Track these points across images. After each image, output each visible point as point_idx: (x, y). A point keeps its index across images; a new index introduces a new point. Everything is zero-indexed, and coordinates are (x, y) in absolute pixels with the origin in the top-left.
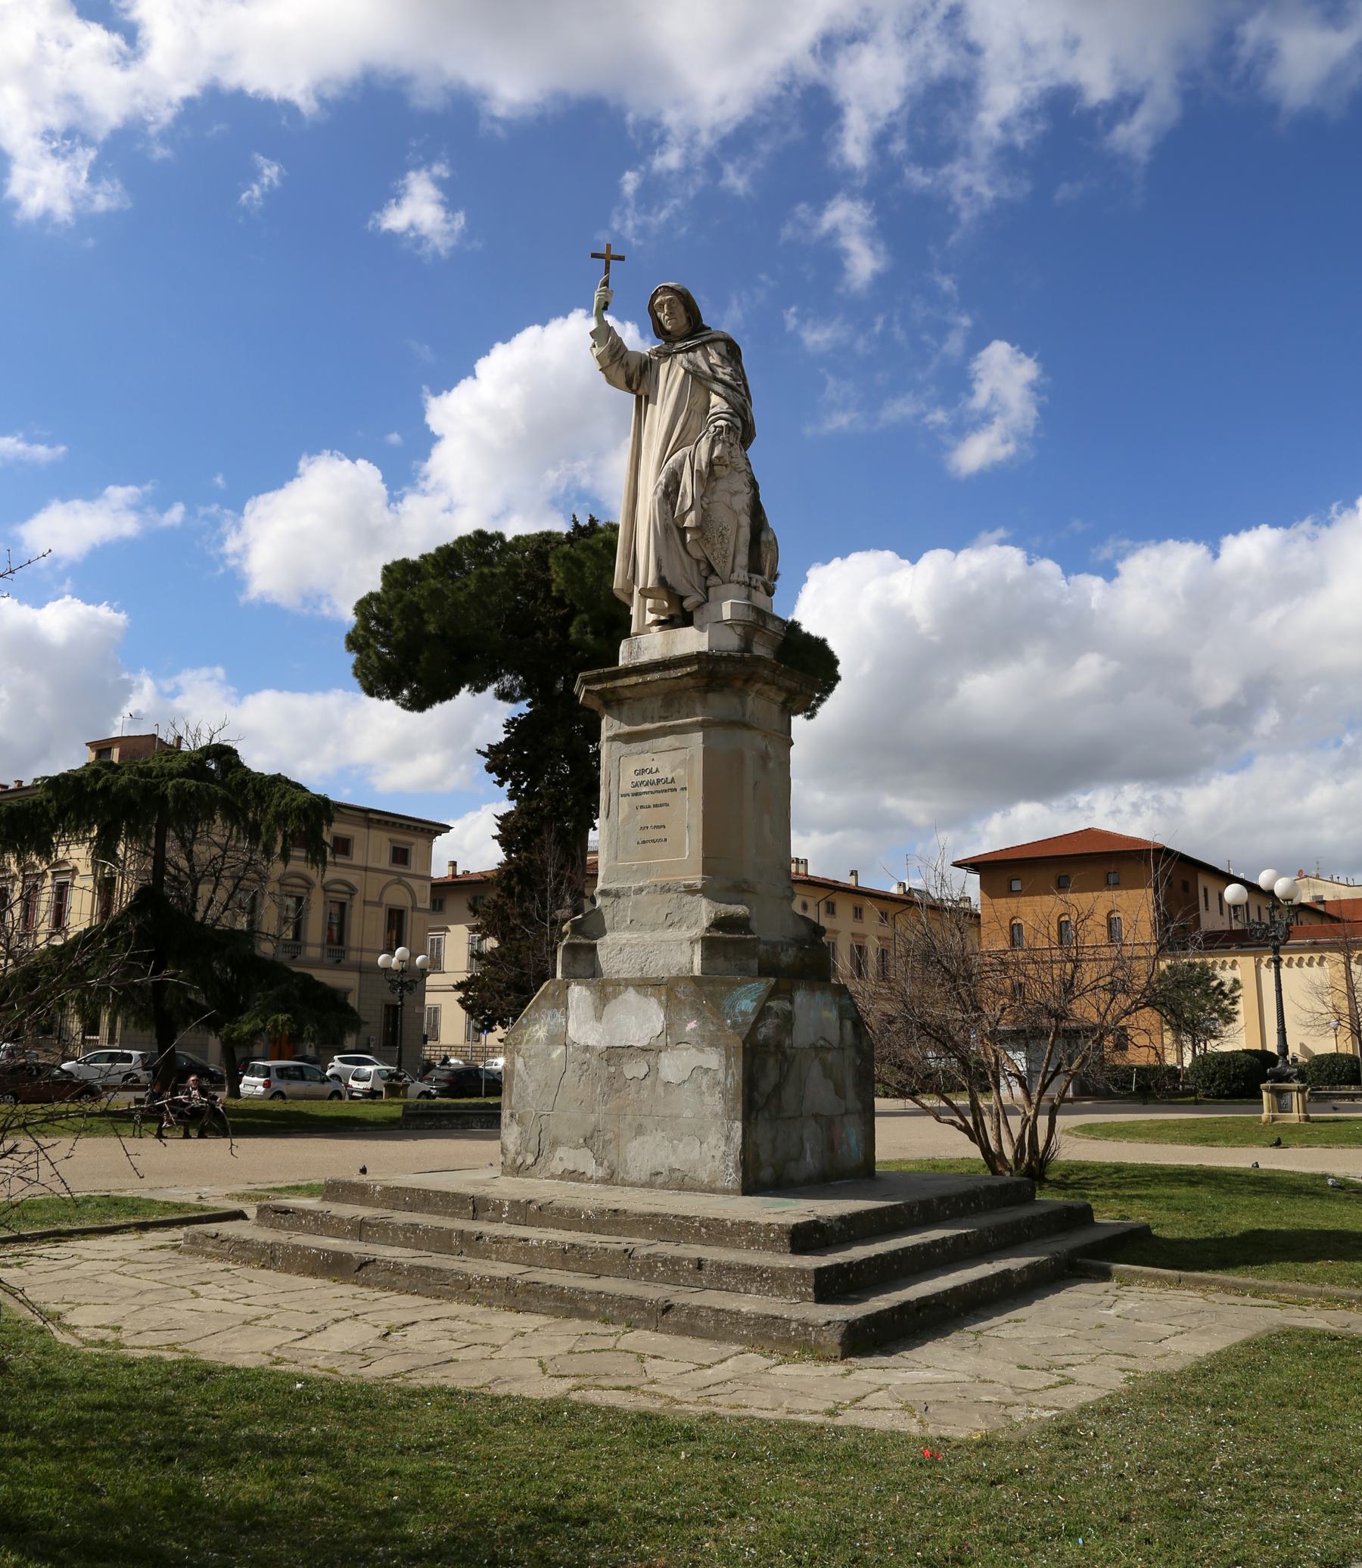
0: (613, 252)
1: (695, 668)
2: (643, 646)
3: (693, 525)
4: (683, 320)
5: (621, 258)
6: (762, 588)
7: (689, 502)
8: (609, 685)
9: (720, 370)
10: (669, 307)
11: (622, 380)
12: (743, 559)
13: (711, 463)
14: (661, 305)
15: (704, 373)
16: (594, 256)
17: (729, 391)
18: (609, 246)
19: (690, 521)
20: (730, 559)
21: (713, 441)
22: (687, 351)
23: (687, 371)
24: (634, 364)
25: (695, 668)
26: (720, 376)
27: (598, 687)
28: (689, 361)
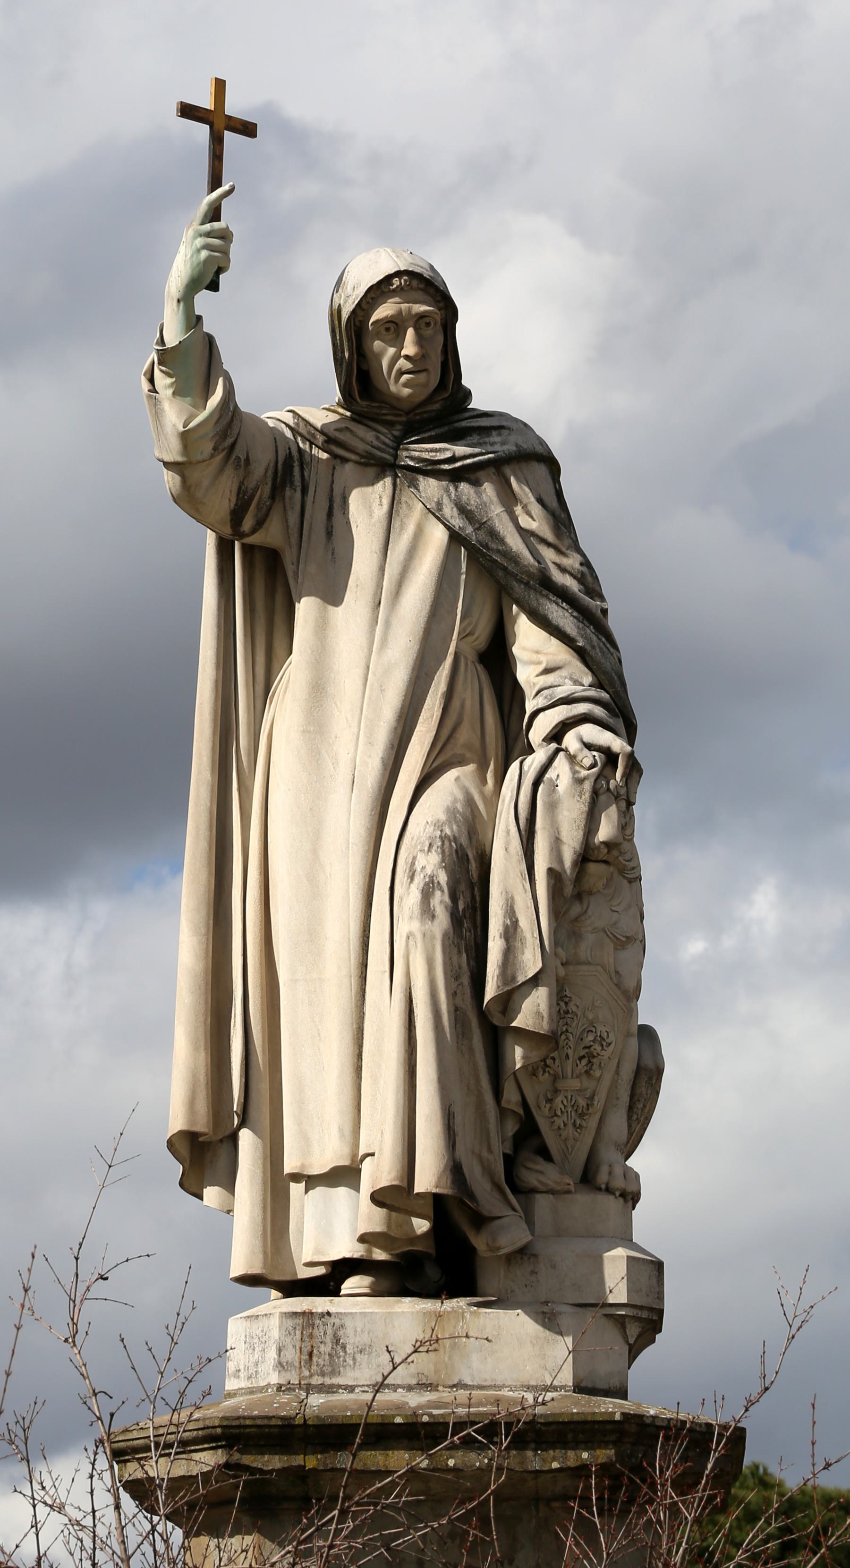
0: (234, 107)
1: (605, 1454)
2: (352, 1339)
3: (544, 1027)
7: (531, 962)
8: (311, 1462)
9: (549, 555)
10: (420, 340)
11: (221, 502)
15: (514, 558)
17: (590, 631)
19: (533, 1011)
20: (592, 1123)
21: (595, 793)
22: (456, 476)
23: (455, 538)
24: (263, 460)
25: (605, 1454)
26: (558, 577)
27: (273, 1462)
28: (463, 510)
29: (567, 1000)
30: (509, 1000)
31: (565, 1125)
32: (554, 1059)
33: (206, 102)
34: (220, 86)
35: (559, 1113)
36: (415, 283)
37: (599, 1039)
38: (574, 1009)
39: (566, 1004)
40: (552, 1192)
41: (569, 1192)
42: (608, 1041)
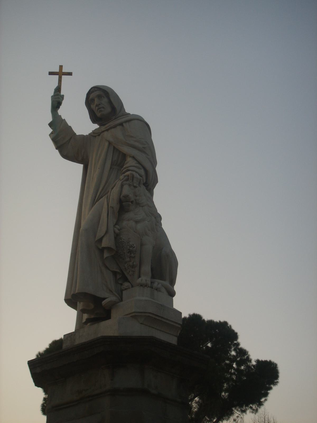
0: (64, 70)
4: (108, 110)
5: (70, 74)
6: (163, 290)
7: (104, 229)
12: (147, 268)
13: (120, 202)
14: (93, 100)
16: (51, 73)
18: (61, 67)
29: (121, 238)
30: (100, 240)
31: (129, 272)
32: (122, 255)
33: (57, 70)
34: (61, 67)
35: (127, 269)
36: (96, 89)
37: (131, 247)
38: (123, 240)
39: (121, 240)
40: (126, 289)
41: (129, 288)
42: (134, 246)
